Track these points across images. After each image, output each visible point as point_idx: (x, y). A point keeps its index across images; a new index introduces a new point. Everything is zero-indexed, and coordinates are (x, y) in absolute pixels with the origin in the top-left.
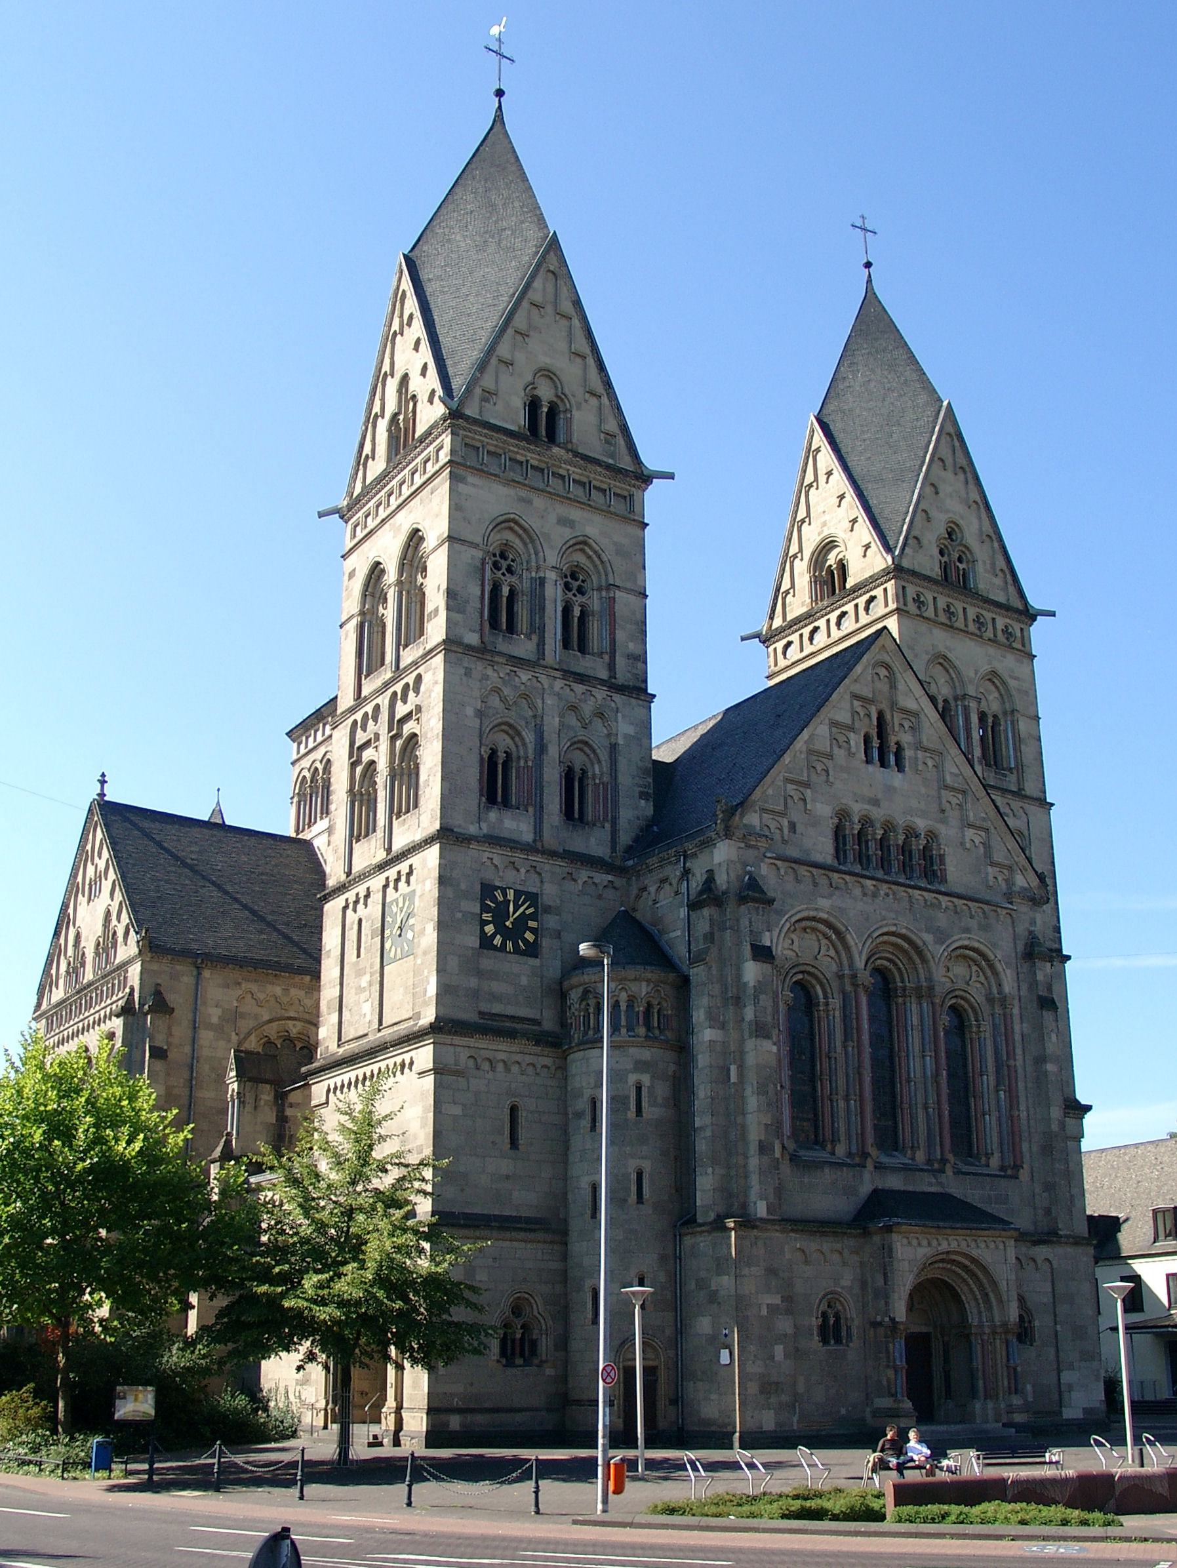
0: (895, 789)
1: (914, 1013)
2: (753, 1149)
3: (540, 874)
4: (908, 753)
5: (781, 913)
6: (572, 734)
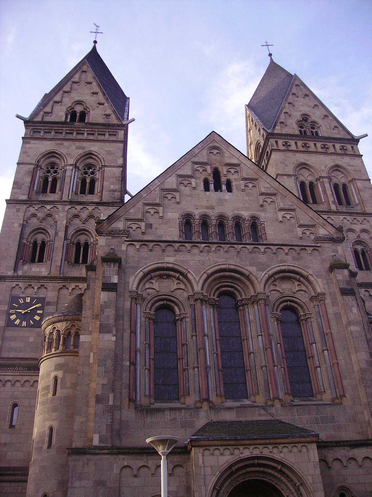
0: (226, 200)
1: (252, 314)
2: (92, 402)
3: (46, 288)
4: (234, 184)
5: (137, 268)
6: (76, 227)
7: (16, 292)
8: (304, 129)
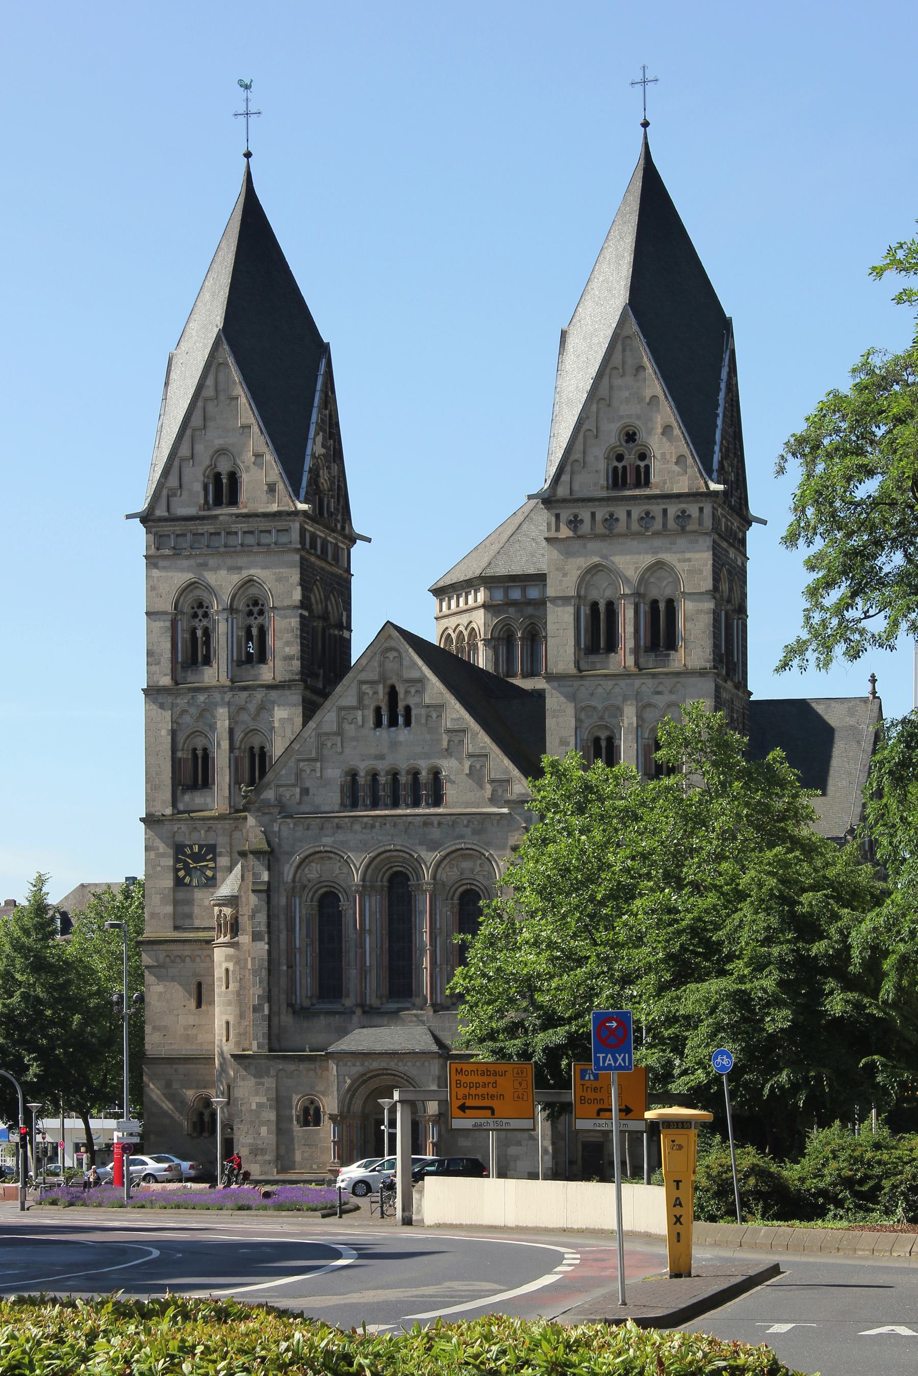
4: (413, 713)
5: (291, 854)
7: (180, 839)
8: (623, 463)
